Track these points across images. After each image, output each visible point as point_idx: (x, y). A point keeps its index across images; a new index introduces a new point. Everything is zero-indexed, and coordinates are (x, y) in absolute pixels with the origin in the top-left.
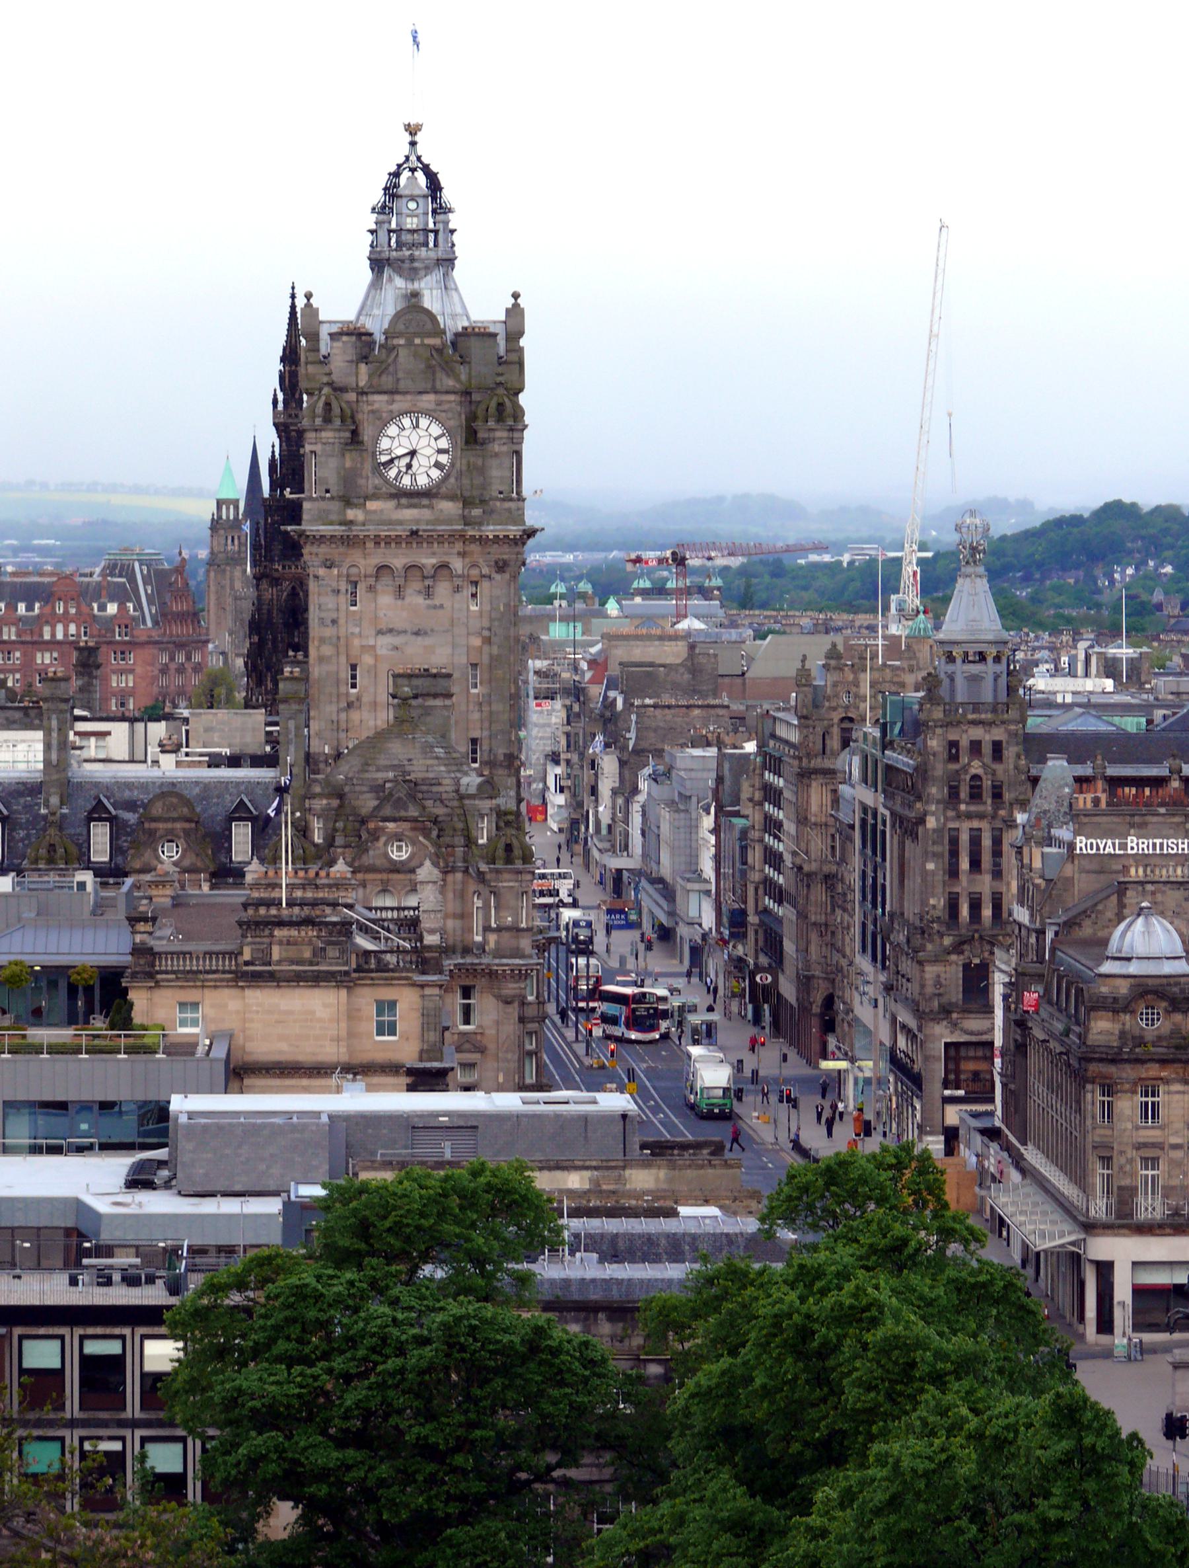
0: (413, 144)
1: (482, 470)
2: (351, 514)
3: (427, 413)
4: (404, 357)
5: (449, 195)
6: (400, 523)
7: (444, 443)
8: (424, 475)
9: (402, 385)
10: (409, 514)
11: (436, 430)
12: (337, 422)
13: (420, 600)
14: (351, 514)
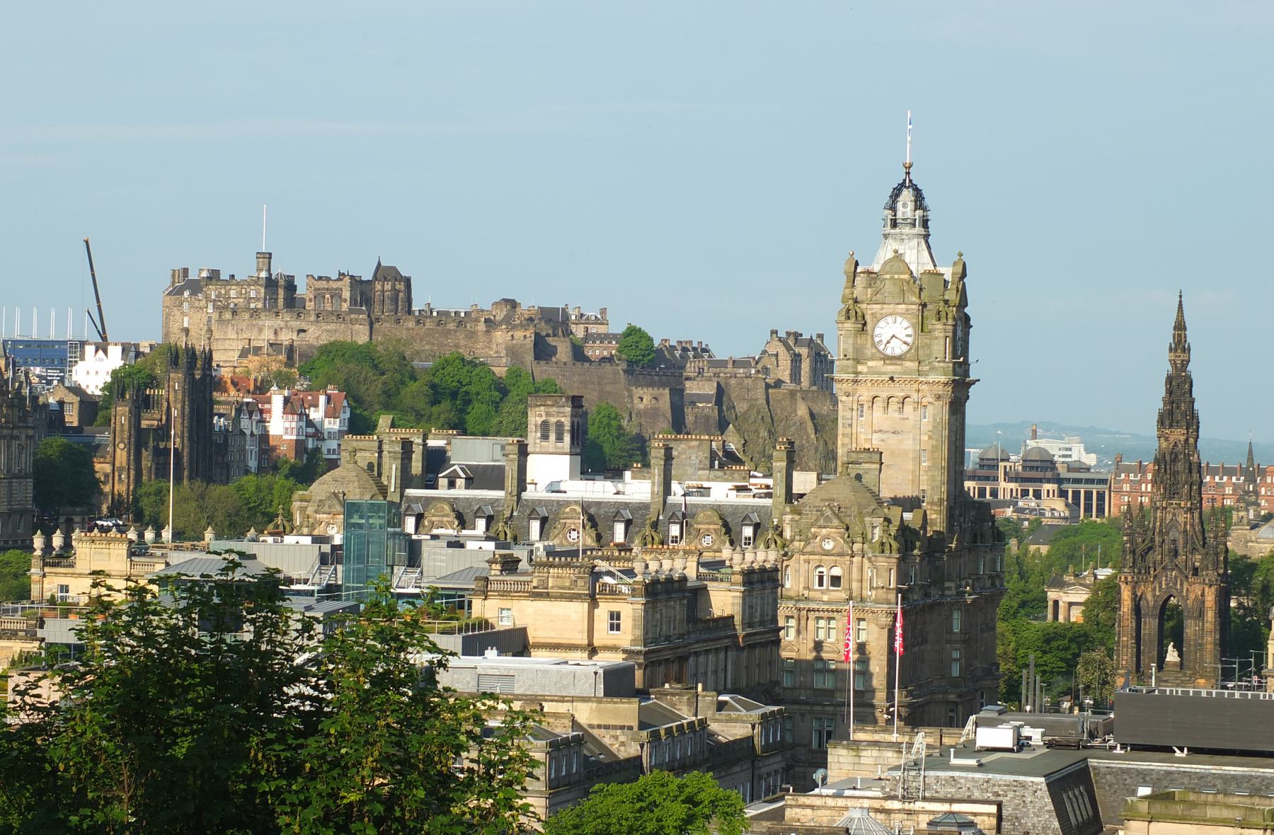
0: (908, 173)
1: (929, 346)
2: (860, 368)
3: (901, 314)
4: (889, 287)
5: (927, 202)
6: (885, 373)
7: (910, 331)
8: (897, 348)
9: (887, 300)
10: (890, 368)
11: (906, 324)
12: (853, 319)
13: (897, 415)
14: (860, 368)
